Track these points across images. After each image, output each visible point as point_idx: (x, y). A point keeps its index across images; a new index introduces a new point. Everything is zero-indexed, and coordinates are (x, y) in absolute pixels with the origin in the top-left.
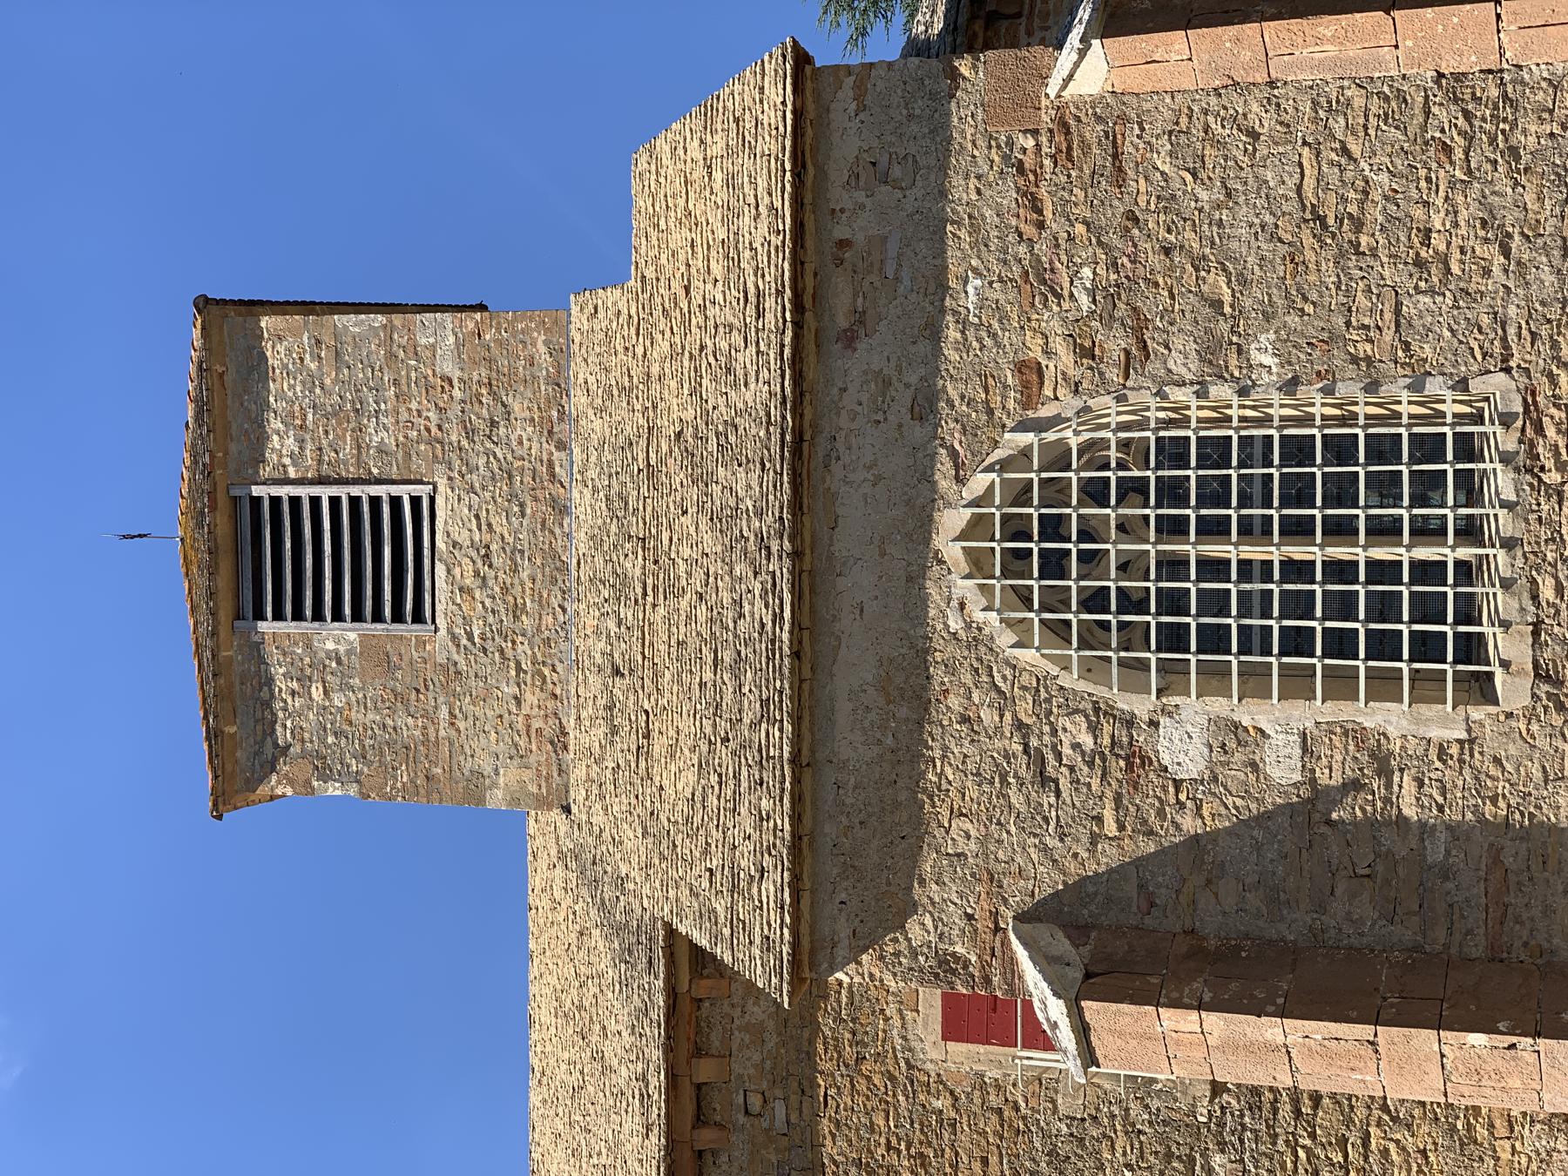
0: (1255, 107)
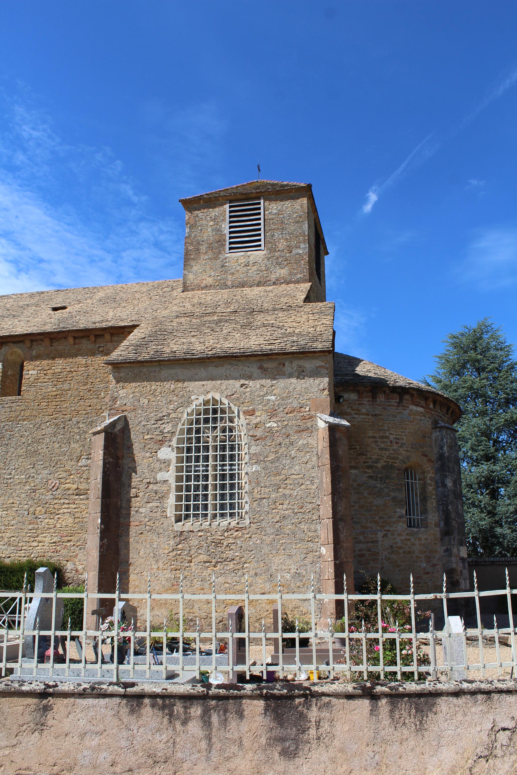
0: (313, 463)
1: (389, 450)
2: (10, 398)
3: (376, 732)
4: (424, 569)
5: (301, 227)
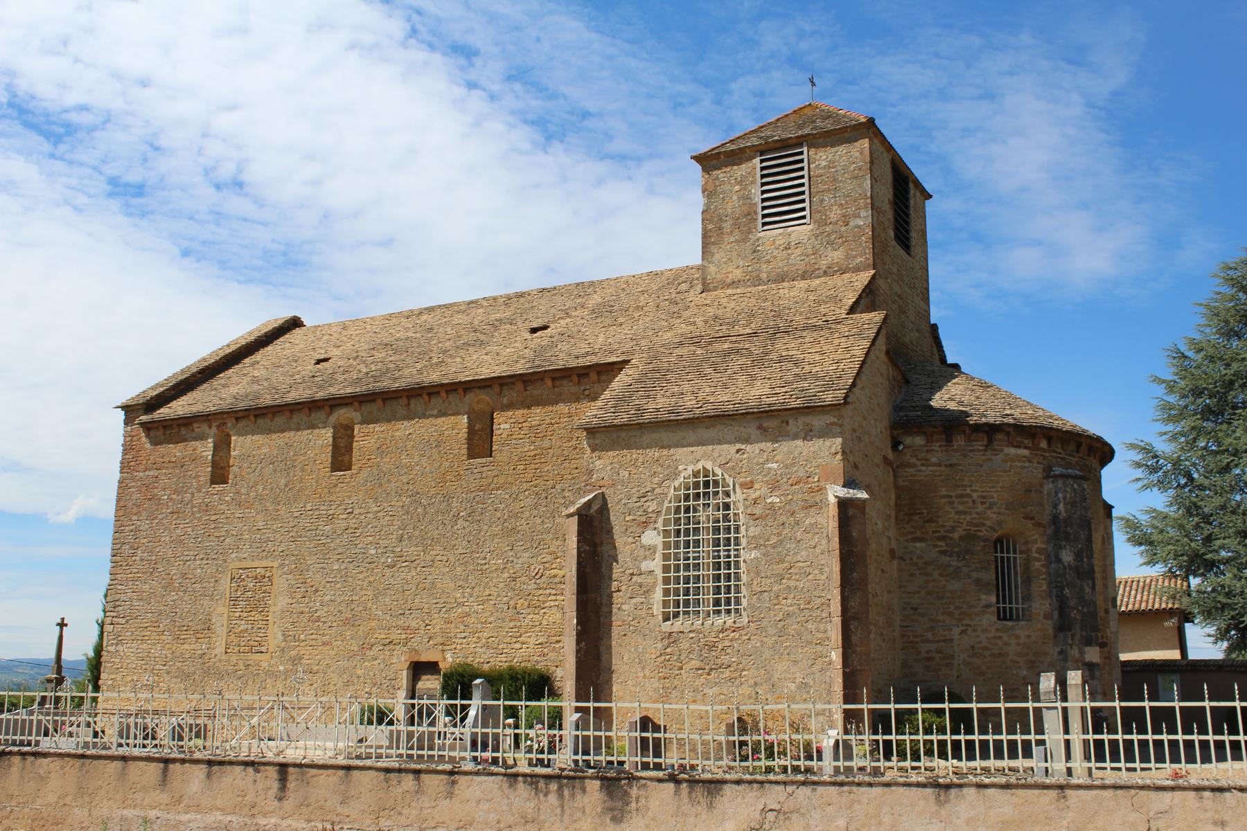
1: (970, 513)
3: (679, 807)
4: (1024, 678)
5: (860, 185)
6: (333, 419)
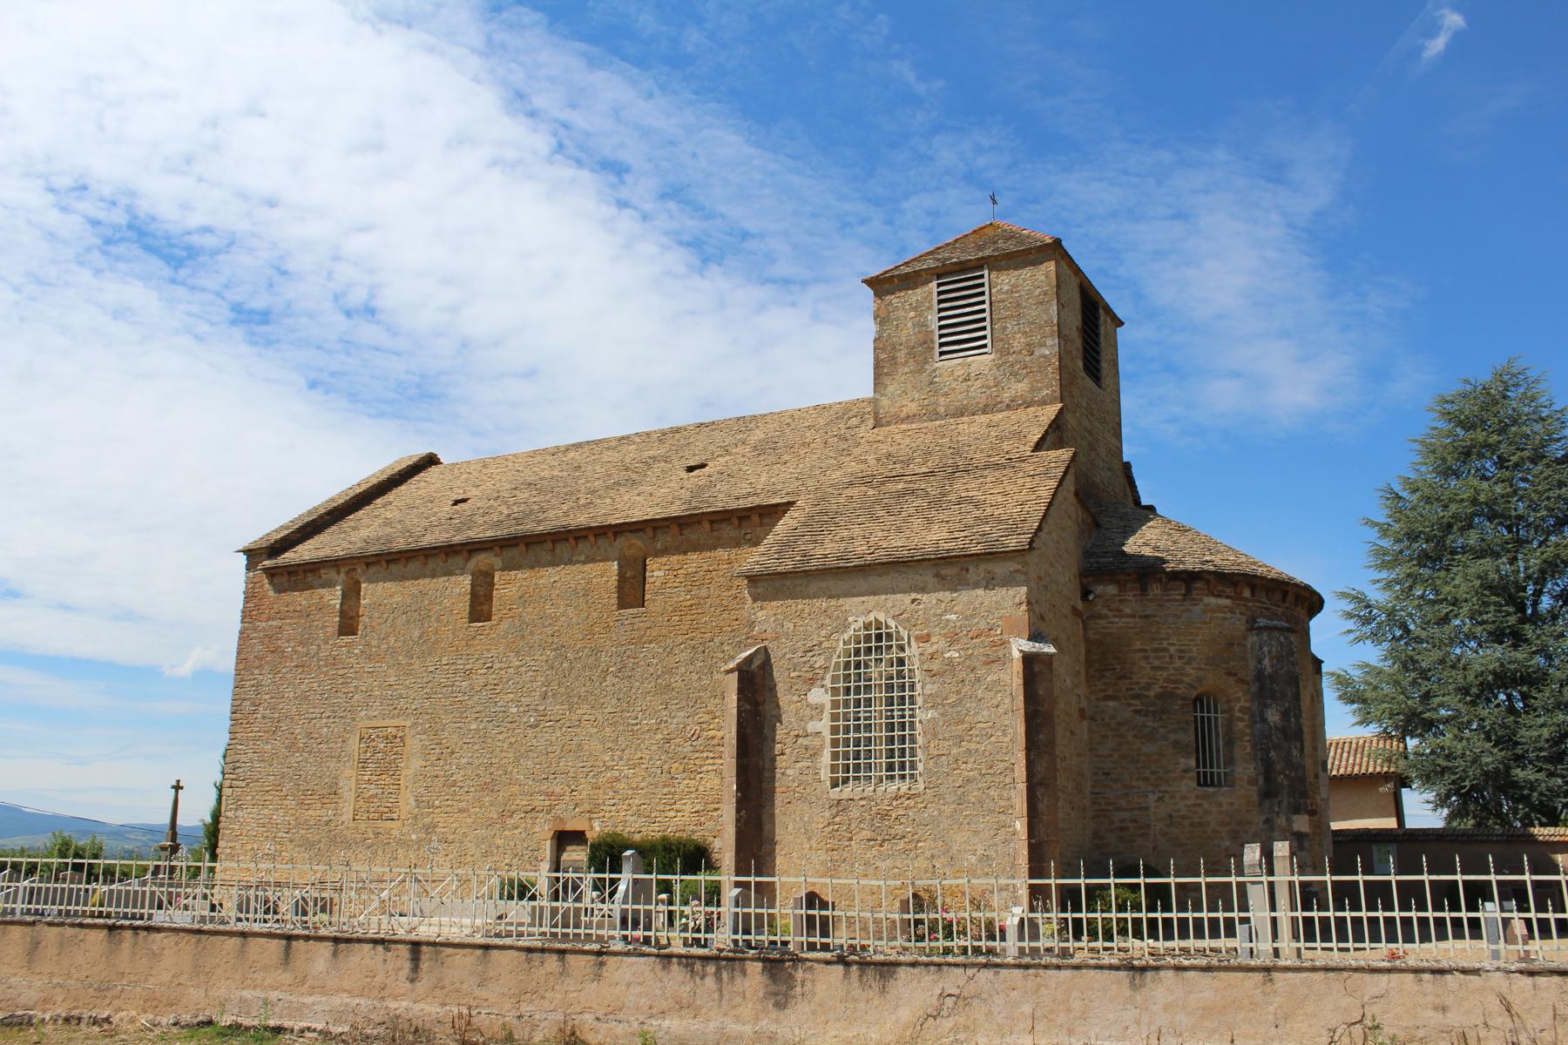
2: (631, 611)
3: (848, 992)
4: (1226, 850)
5: (1046, 311)
6: (471, 565)
